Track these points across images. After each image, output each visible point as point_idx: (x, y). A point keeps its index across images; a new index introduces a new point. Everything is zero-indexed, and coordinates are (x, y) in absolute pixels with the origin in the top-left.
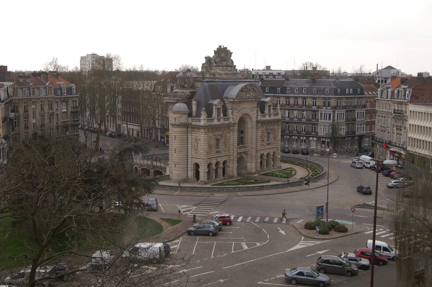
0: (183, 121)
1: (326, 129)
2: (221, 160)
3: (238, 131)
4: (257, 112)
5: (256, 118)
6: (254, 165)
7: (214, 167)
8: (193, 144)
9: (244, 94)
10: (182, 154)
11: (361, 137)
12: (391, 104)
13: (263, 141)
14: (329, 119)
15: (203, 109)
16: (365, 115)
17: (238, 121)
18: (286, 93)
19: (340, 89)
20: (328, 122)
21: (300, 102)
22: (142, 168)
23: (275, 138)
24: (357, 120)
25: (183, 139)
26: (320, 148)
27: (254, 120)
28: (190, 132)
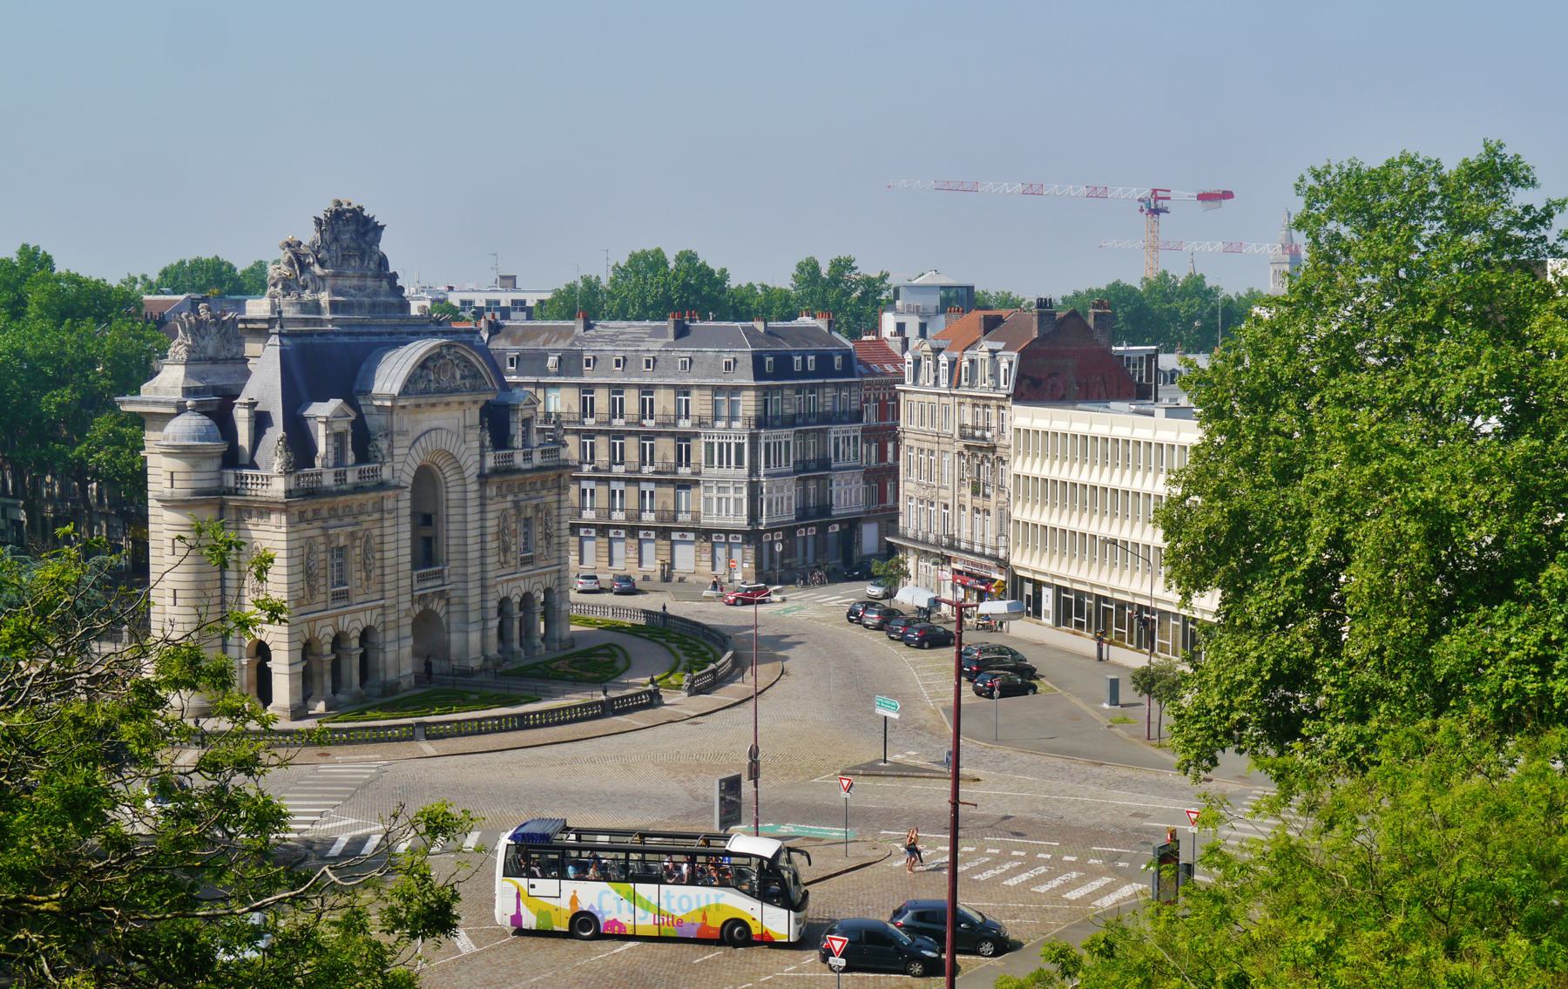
1: (728, 499)
3: (413, 515)
5: (478, 465)
6: (475, 638)
12: (951, 406)
13: (505, 549)
17: (410, 481)
18: (581, 374)
23: (548, 536)
27: (472, 471)
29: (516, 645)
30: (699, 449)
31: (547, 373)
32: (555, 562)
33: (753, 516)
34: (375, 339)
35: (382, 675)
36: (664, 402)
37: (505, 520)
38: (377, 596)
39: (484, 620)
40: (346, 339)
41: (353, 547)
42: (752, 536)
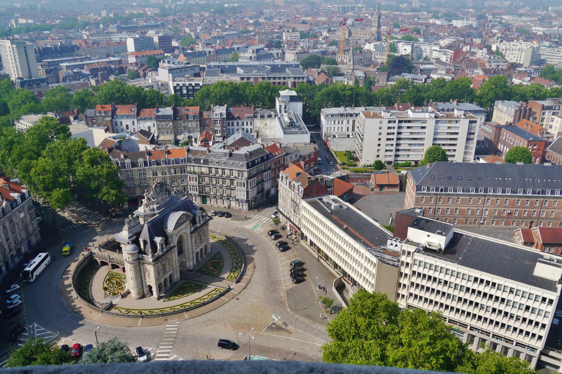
6: (191, 263)
13: (196, 243)
18: (208, 164)
23: (205, 236)
29: (200, 259)
30: (235, 183)
31: (201, 164)
33: (247, 197)
36: (227, 172)
39: (193, 259)
42: (247, 201)
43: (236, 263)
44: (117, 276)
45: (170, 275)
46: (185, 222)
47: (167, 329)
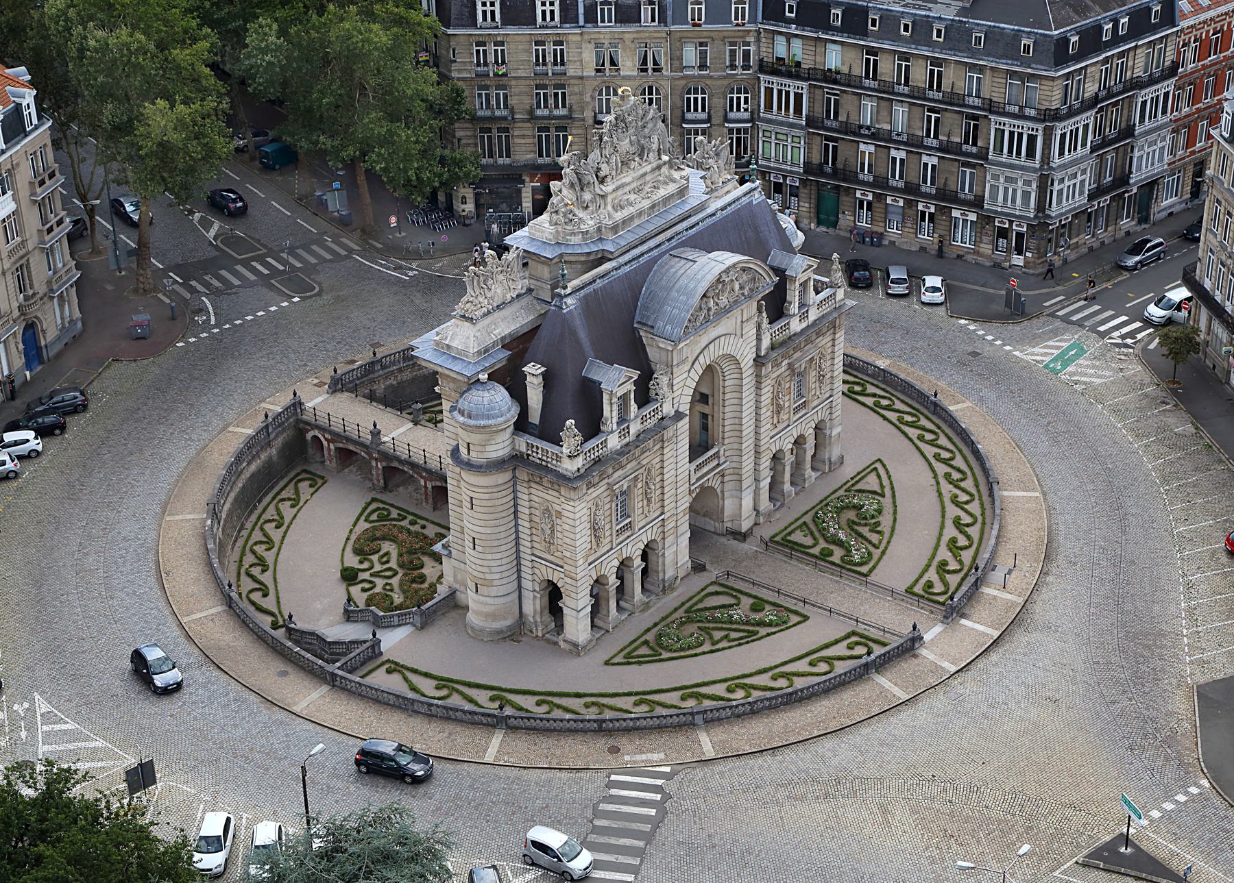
0: (500, 454)
2: (634, 549)
4: (759, 326)
5: (754, 349)
6: (747, 501)
7: (613, 581)
8: (537, 520)
9: (711, 304)
10: (499, 556)
11: (1150, 187)
13: (778, 410)
14: (1027, 155)
15: (568, 423)
16: (1174, 95)
18: (864, 34)
19: (1078, 33)
20: (1022, 168)
21: (920, 75)
22: (341, 445)
23: (821, 378)
24: (1138, 129)
25: (501, 508)
26: (990, 252)
28: (525, 485)
31: (828, 28)
32: (827, 395)
34: (655, 253)
35: (661, 575)
37: (780, 384)
38: (658, 513)
40: (627, 269)
41: (636, 486)
43: (957, 523)
44: (405, 523)
45: (646, 546)
46: (736, 303)
47: (614, 792)
